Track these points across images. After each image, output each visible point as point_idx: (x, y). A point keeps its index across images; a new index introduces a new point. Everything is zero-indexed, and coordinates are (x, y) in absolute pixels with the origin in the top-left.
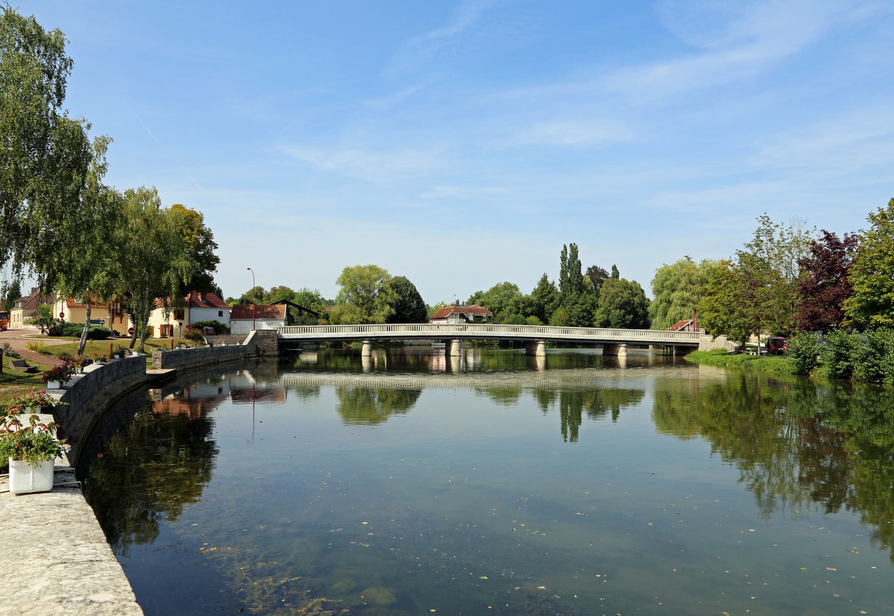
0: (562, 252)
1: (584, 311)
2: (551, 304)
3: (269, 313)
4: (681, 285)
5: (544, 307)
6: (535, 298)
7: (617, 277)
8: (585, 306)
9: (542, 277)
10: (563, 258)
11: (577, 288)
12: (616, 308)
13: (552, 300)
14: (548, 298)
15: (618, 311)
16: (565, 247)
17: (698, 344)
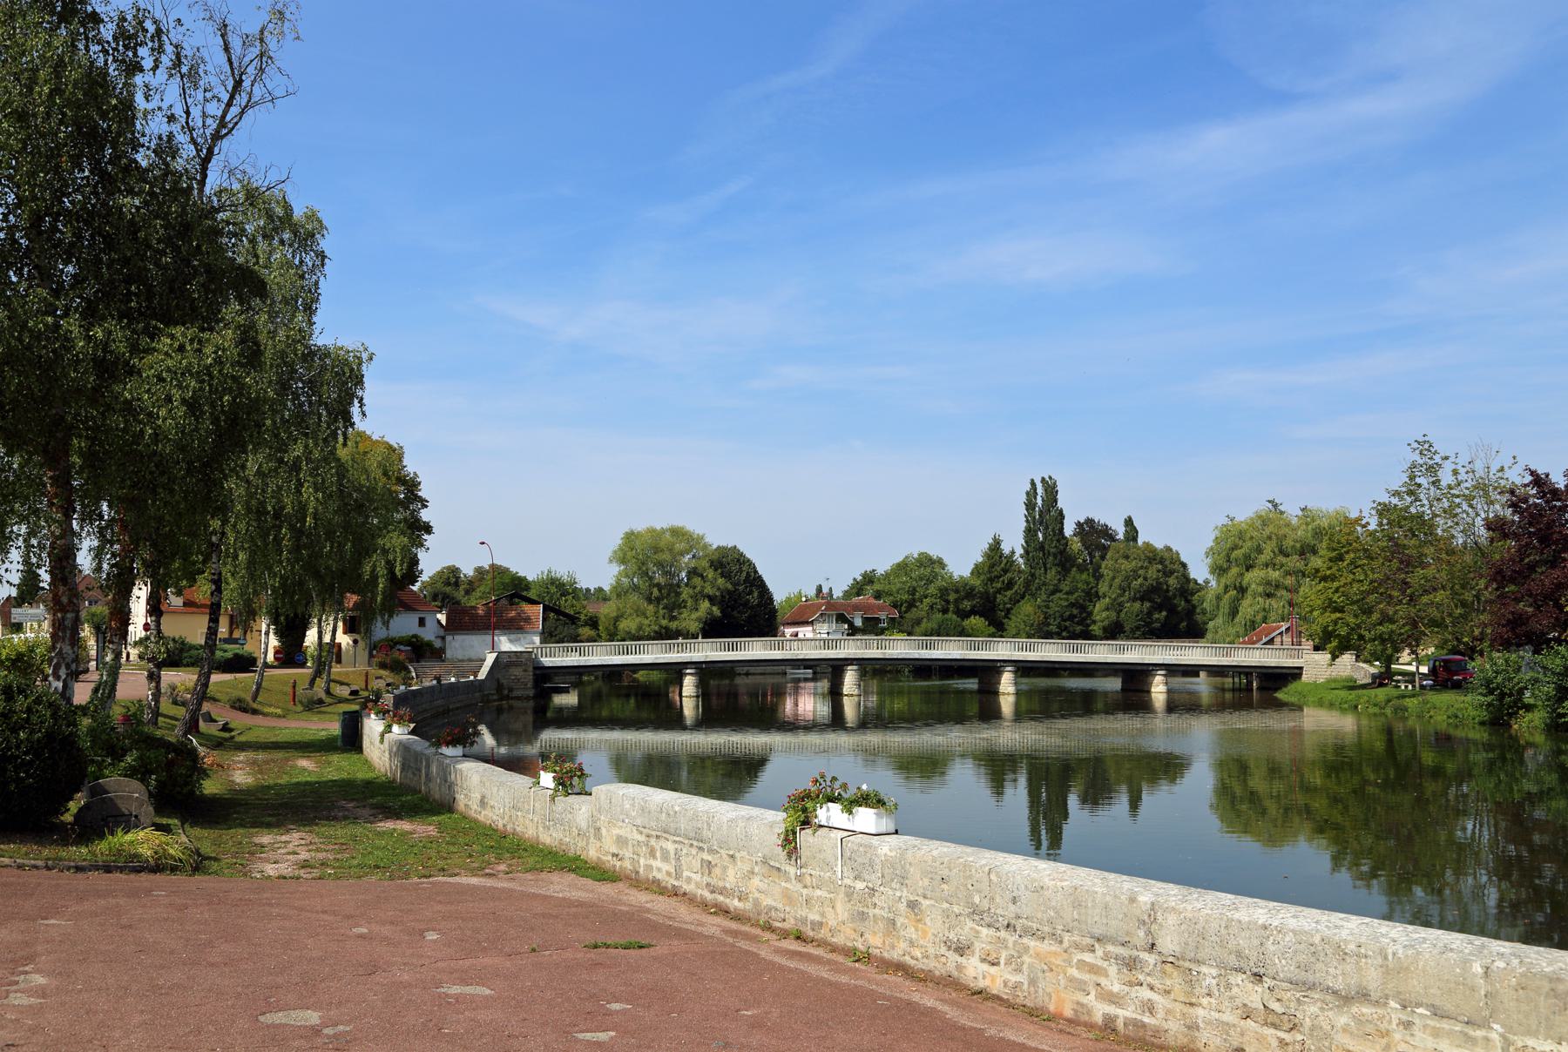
0: (1028, 493)
1: (1072, 605)
2: (1009, 593)
3: (512, 620)
4: (1263, 558)
5: (995, 598)
6: (977, 582)
7: (1135, 539)
8: (1075, 596)
9: (991, 541)
10: (1030, 506)
11: (1057, 561)
12: (1134, 600)
13: (1010, 585)
14: (1003, 582)
15: (1137, 605)
16: (1033, 483)
17: (1301, 668)
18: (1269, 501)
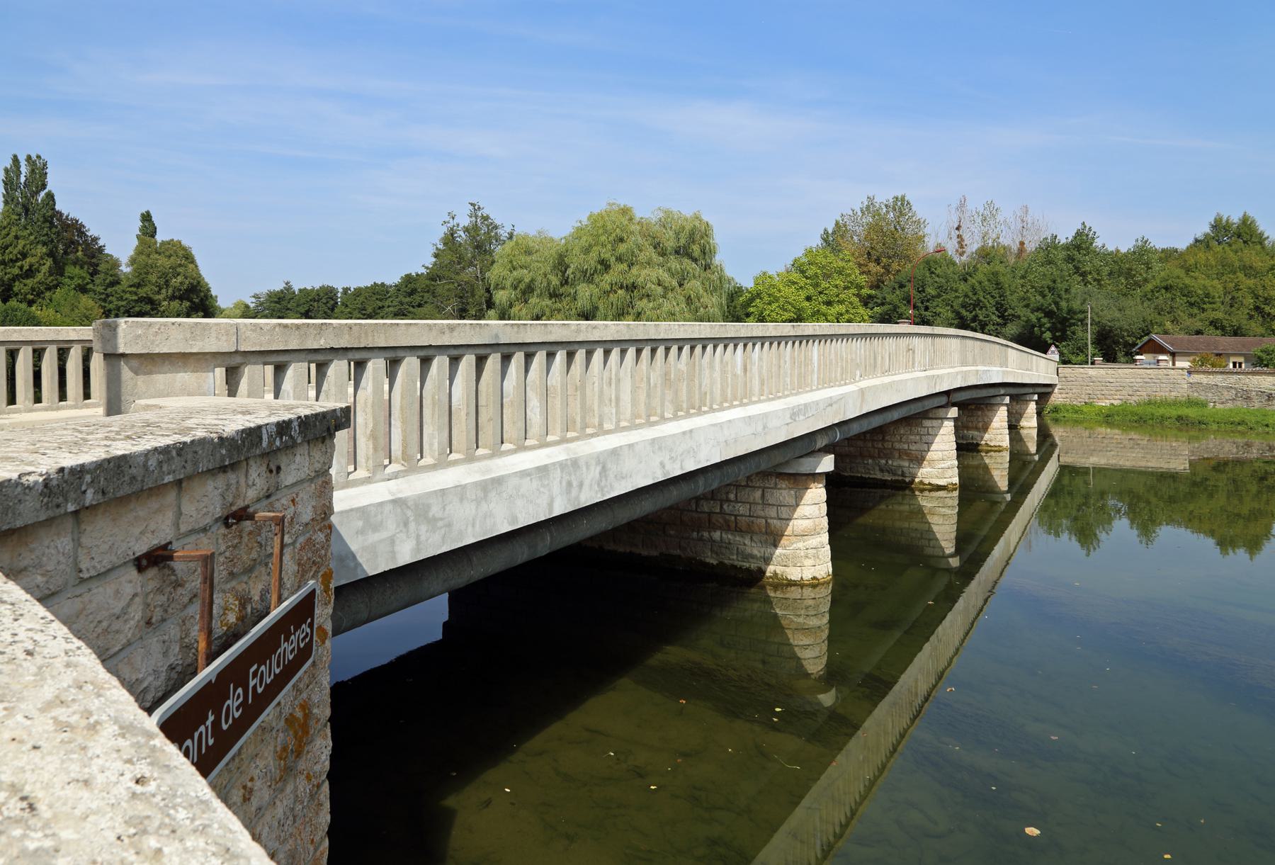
2: (30, 282)
7: (153, 233)
10: (9, 184)
12: (173, 298)
13: (30, 273)
14: (21, 268)
18: (472, 204)
